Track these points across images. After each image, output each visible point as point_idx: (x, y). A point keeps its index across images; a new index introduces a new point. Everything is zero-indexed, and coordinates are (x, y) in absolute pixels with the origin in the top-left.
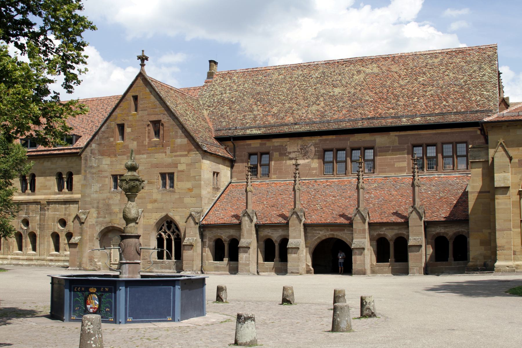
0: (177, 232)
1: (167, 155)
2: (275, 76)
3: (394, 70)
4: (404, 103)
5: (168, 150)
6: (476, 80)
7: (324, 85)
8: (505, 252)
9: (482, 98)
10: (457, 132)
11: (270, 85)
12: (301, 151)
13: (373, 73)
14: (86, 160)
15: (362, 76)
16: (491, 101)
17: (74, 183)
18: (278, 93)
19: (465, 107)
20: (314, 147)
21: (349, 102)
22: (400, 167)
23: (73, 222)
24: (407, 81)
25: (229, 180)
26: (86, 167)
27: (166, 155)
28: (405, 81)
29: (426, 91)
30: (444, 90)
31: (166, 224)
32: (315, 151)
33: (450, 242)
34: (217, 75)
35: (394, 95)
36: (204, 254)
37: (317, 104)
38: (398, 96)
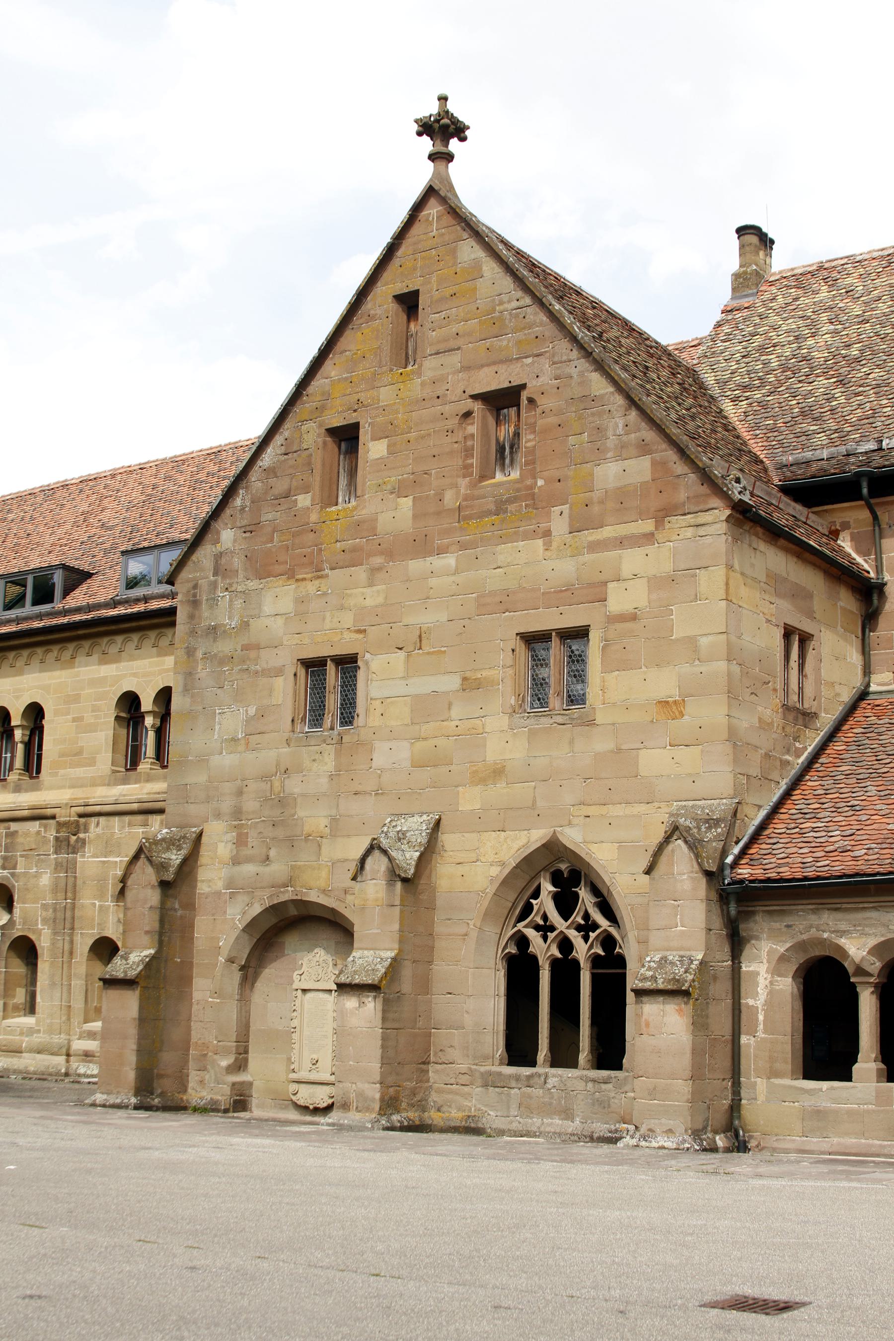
0: (603, 923)
1: (555, 545)
14: (195, 603)
25: (858, 681)
26: (193, 632)
27: (547, 547)
31: (547, 888)
34: (772, 284)
36: (744, 1039)
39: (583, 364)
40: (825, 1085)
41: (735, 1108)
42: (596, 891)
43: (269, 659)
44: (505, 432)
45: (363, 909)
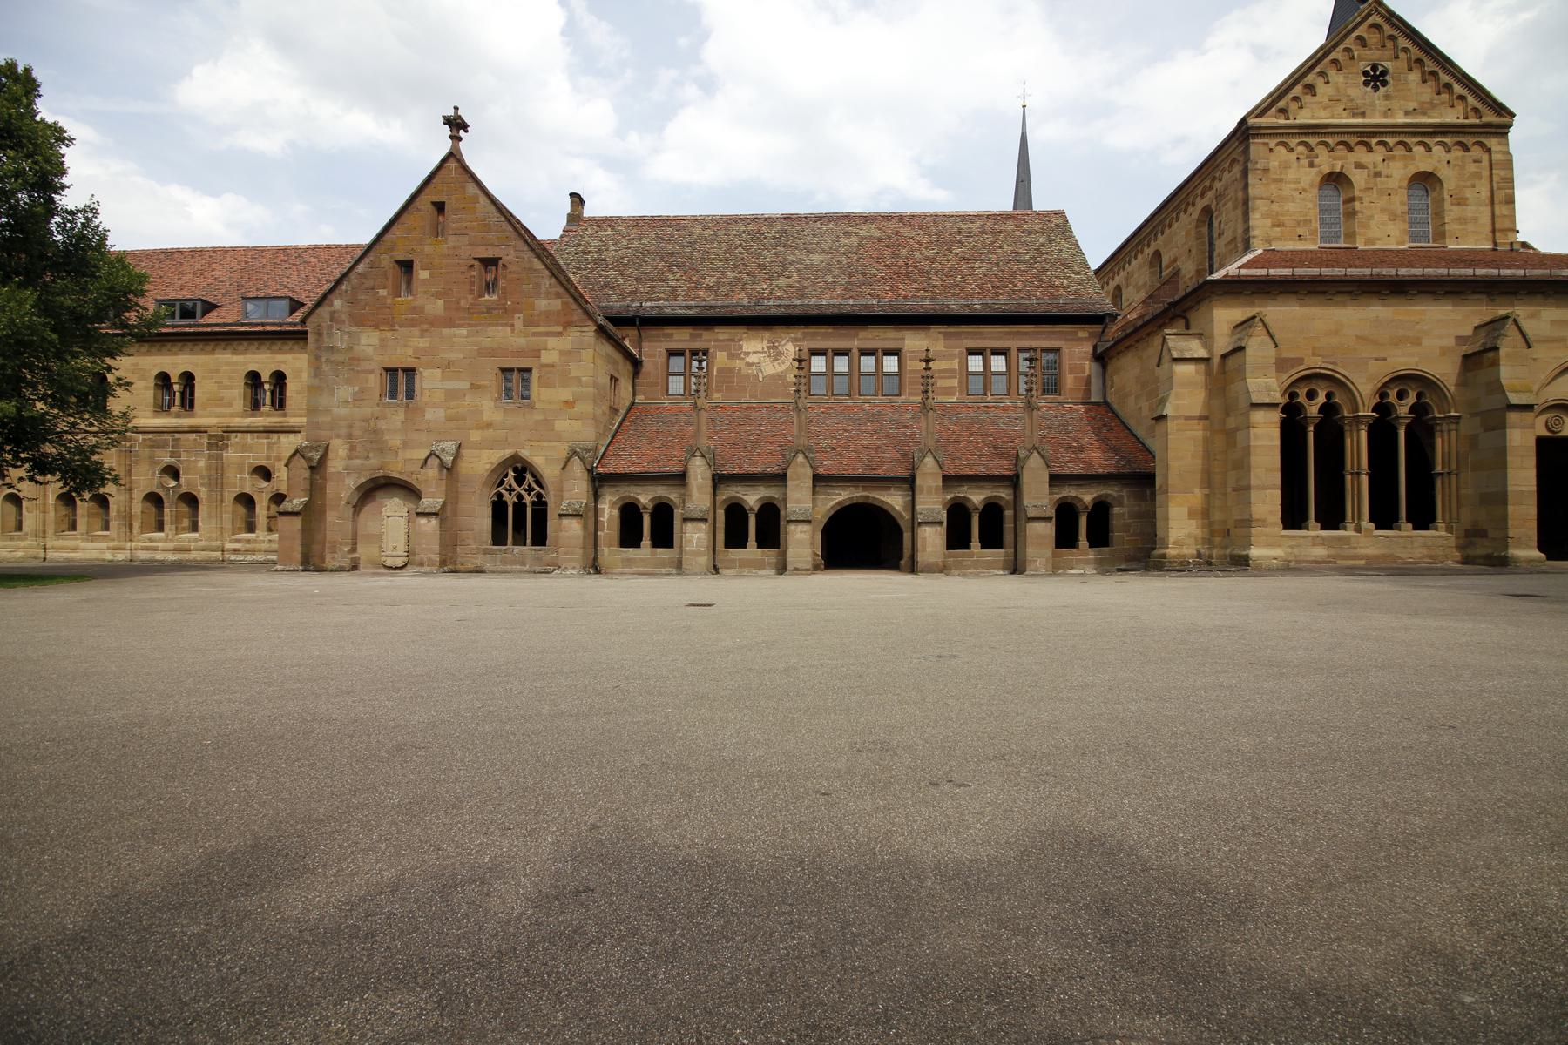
0: (538, 489)
2: (698, 230)
5: (518, 321)
8: (1267, 530)
14: (319, 334)
15: (854, 240)
17: (288, 394)
21: (843, 276)
23: (286, 465)
26: (319, 348)
27: (513, 331)
31: (511, 474)
34: (585, 222)
36: (599, 533)
38: (928, 273)
39: (530, 254)
40: (631, 549)
41: (595, 559)
42: (533, 475)
43: (365, 365)
44: (490, 277)
45: (426, 481)
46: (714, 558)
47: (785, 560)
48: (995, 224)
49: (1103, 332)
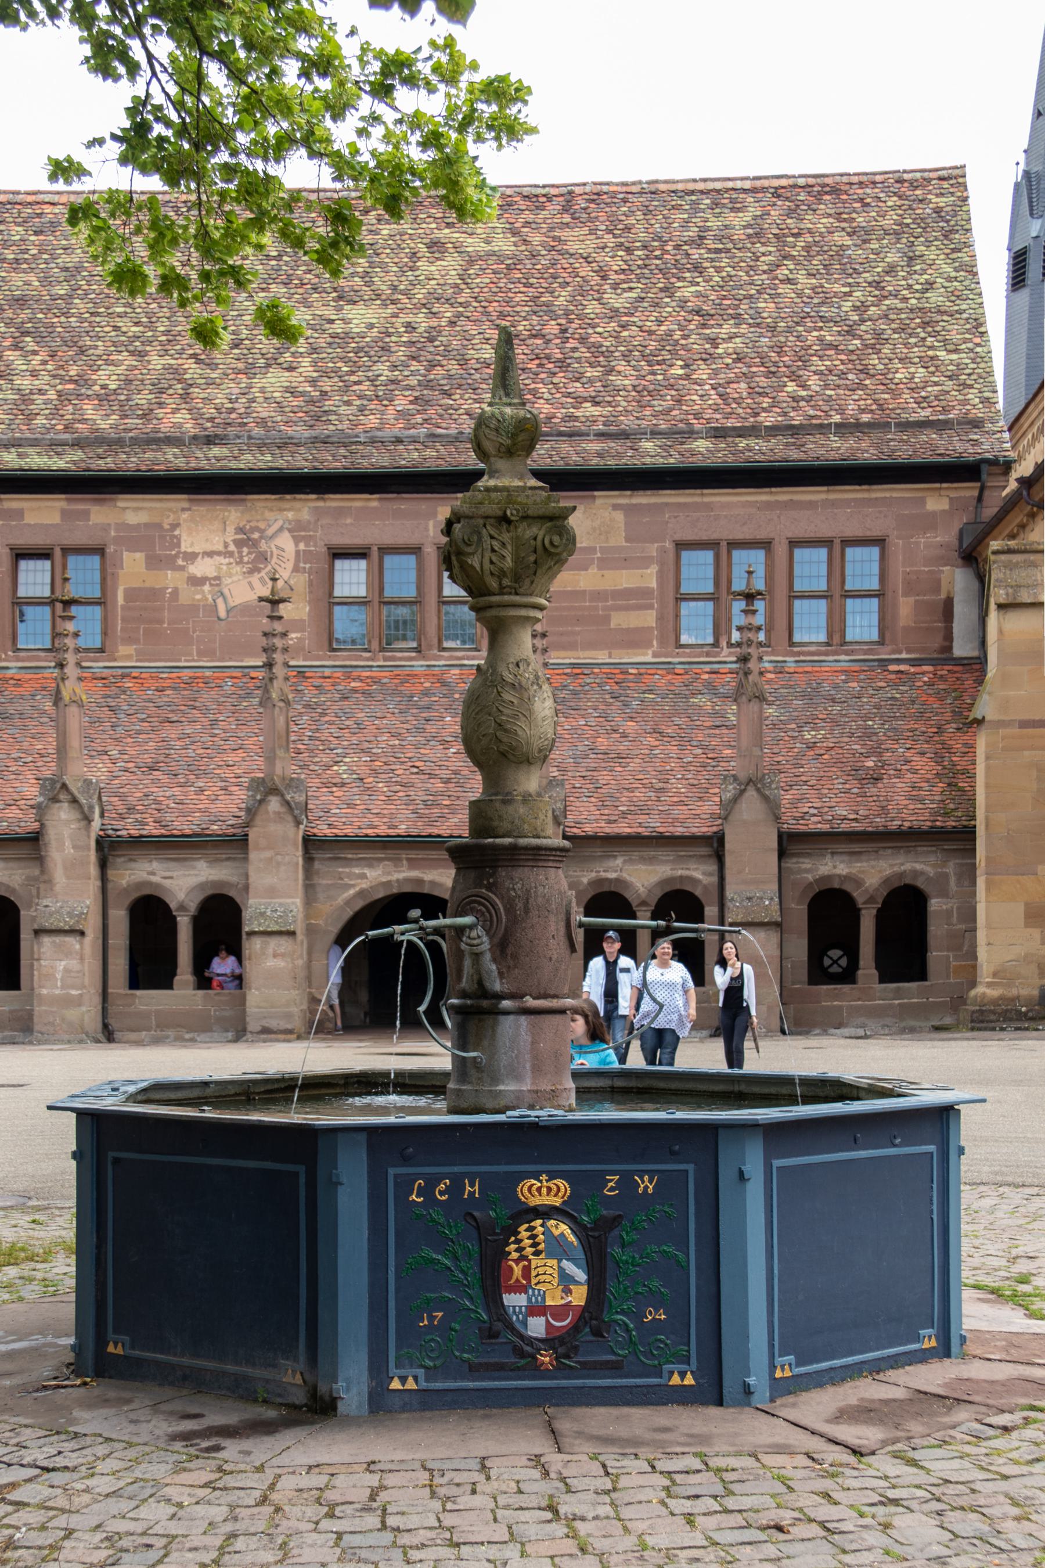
3: (574, 247)
4: (636, 383)
6: (900, 306)
7: (300, 291)
9: (933, 373)
10: (847, 503)
11: (66, 269)
12: (240, 553)
13: (493, 254)
15: (450, 265)
16: (971, 387)
18: (108, 308)
19: (874, 407)
20: (293, 537)
21: (415, 366)
22: (628, 631)
24: (632, 295)
28: (626, 295)
29: (714, 342)
30: (783, 339)
32: (298, 552)
33: (863, 912)
35: (593, 350)
37: (285, 365)
38: (608, 354)
46: (104, 1011)
47: (244, 1012)
48: (790, 213)
49: (980, 499)
